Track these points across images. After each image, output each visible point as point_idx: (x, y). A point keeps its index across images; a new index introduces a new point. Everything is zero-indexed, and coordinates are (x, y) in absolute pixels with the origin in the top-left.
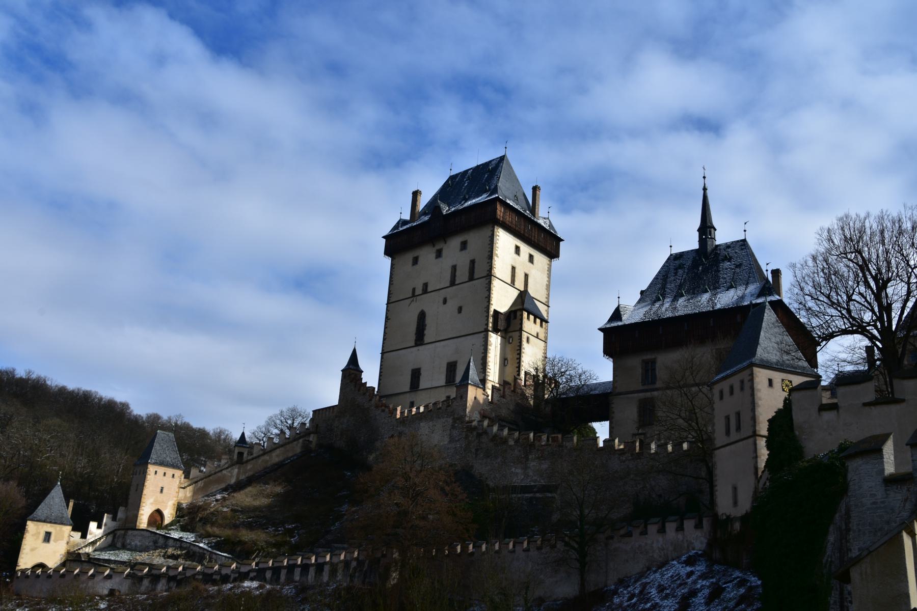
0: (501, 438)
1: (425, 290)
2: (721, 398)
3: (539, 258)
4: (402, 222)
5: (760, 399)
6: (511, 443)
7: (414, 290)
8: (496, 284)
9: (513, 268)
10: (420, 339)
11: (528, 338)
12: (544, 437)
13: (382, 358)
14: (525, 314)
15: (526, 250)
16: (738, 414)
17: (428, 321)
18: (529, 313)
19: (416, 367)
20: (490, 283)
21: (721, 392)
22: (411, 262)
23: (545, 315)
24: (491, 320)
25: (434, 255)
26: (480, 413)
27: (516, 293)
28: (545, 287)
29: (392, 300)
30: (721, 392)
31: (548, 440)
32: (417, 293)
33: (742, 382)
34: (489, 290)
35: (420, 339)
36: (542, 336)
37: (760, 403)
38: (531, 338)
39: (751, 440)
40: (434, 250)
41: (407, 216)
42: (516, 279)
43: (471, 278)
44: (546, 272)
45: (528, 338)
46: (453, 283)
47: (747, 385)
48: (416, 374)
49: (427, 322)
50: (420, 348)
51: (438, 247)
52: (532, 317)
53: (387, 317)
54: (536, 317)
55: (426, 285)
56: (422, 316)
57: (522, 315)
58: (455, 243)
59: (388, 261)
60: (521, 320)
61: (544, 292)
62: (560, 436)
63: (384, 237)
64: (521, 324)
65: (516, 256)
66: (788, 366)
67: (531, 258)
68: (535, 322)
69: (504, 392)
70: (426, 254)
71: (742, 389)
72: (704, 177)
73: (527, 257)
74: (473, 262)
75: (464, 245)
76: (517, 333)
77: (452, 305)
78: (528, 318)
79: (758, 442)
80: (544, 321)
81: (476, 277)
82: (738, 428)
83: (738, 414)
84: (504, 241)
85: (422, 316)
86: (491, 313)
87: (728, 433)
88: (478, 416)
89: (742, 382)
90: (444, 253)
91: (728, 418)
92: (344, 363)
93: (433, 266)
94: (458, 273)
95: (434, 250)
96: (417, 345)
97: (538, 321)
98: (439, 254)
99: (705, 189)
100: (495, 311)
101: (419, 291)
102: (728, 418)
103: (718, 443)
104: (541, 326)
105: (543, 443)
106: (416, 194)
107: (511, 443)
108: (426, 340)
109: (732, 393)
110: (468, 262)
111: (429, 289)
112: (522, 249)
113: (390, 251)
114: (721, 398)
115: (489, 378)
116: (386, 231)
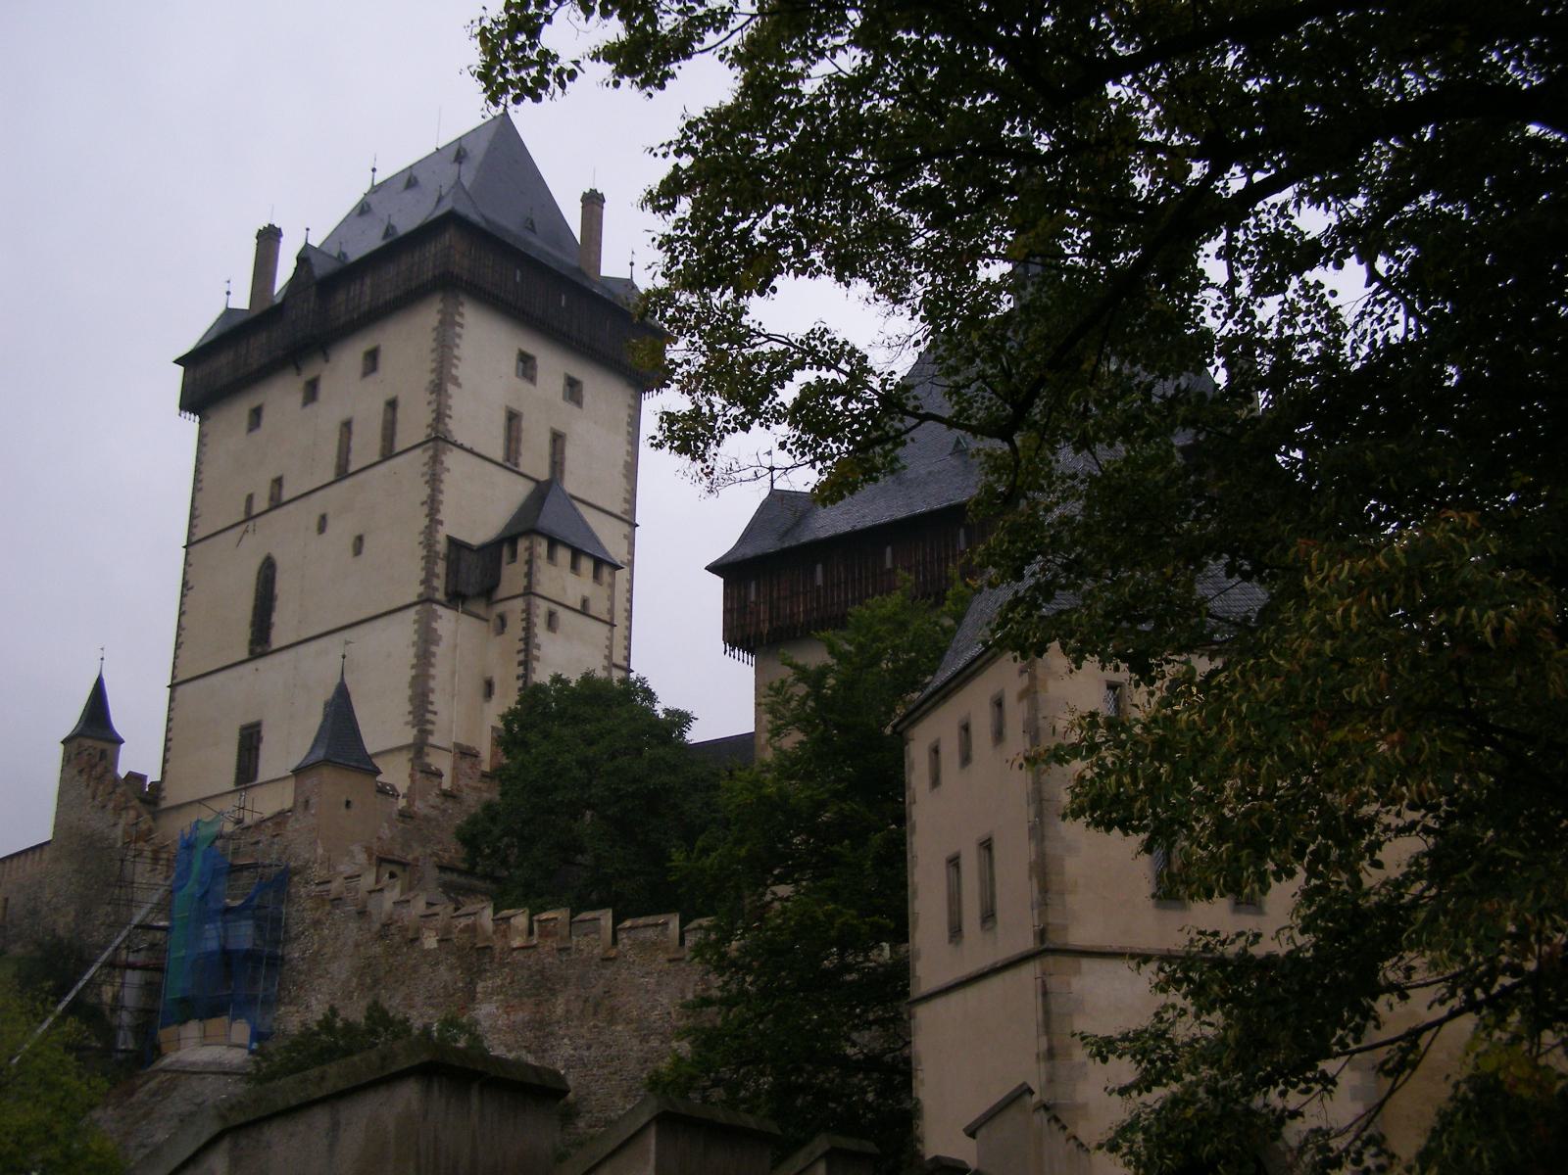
0: (403, 929)
1: (276, 503)
2: (935, 781)
3: (603, 391)
4: (229, 312)
6: (430, 942)
7: (250, 498)
8: (453, 459)
9: (513, 418)
10: (260, 641)
11: (551, 615)
12: (520, 920)
13: (171, 699)
14: (542, 548)
15: (553, 365)
16: (987, 845)
17: (283, 585)
18: (553, 543)
19: (251, 719)
20: (435, 460)
21: (935, 751)
22: (244, 424)
23: (616, 551)
24: (441, 568)
25: (299, 397)
26: (368, 850)
27: (521, 490)
28: (620, 468)
29: (200, 534)
30: (935, 751)
31: (531, 932)
32: (256, 510)
33: (999, 704)
34: (434, 481)
35: (260, 641)
36: (598, 607)
38: (562, 613)
39: (1029, 972)
41: (242, 301)
42: (524, 449)
43: (388, 453)
44: (624, 428)
45: (551, 615)
46: (343, 473)
47: (1016, 714)
48: (250, 740)
49: (277, 591)
50: (261, 663)
51: (308, 374)
52: (563, 555)
53: (185, 584)
54: (577, 553)
55: (278, 482)
56: (267, 573)
57: (530, 550)
58: (349, 357)
59: (191, 424)
60: (530, 563)
61: (623, 483)
62: (561, 914)
64: (529, 575)
65: (523, 385)
67: (573, 387)
68: (574, 567)
69: (455, 778)
70: (281, 396)
71: (999, 735)
73: (559, 385)
74: (392, 405)
75: (372, 359)
77: (341, 531)
78: (551, 556)
79: (1053, 983)
80: (603, 565)
81: (399, 447)
82: (988, 916)
83: (987, 845)
84: (486, 346)
85: (267, 573)
86: (442, 547)
87: (956, 932)
88: (362, 857)
89: (999, 704)
91: (954, 862)
92: (70, 717)
93: (295, 424)
94: (356, 443)
96: (254, 656)
97: (586, 565)
98: (311, 392)
100: (452, 542)
102: (954, 862)
103: (927, 974)
104: (596, 576)
105: (517, 942)
106: (269, 237)
107: (430, 942)
108: (278, 639)
109: (966, 759)
111: (286, 497)
112: (540, 362)
113: (198, 399)
114: (935, 781)
115: (432, 740)
116: (188, 344)
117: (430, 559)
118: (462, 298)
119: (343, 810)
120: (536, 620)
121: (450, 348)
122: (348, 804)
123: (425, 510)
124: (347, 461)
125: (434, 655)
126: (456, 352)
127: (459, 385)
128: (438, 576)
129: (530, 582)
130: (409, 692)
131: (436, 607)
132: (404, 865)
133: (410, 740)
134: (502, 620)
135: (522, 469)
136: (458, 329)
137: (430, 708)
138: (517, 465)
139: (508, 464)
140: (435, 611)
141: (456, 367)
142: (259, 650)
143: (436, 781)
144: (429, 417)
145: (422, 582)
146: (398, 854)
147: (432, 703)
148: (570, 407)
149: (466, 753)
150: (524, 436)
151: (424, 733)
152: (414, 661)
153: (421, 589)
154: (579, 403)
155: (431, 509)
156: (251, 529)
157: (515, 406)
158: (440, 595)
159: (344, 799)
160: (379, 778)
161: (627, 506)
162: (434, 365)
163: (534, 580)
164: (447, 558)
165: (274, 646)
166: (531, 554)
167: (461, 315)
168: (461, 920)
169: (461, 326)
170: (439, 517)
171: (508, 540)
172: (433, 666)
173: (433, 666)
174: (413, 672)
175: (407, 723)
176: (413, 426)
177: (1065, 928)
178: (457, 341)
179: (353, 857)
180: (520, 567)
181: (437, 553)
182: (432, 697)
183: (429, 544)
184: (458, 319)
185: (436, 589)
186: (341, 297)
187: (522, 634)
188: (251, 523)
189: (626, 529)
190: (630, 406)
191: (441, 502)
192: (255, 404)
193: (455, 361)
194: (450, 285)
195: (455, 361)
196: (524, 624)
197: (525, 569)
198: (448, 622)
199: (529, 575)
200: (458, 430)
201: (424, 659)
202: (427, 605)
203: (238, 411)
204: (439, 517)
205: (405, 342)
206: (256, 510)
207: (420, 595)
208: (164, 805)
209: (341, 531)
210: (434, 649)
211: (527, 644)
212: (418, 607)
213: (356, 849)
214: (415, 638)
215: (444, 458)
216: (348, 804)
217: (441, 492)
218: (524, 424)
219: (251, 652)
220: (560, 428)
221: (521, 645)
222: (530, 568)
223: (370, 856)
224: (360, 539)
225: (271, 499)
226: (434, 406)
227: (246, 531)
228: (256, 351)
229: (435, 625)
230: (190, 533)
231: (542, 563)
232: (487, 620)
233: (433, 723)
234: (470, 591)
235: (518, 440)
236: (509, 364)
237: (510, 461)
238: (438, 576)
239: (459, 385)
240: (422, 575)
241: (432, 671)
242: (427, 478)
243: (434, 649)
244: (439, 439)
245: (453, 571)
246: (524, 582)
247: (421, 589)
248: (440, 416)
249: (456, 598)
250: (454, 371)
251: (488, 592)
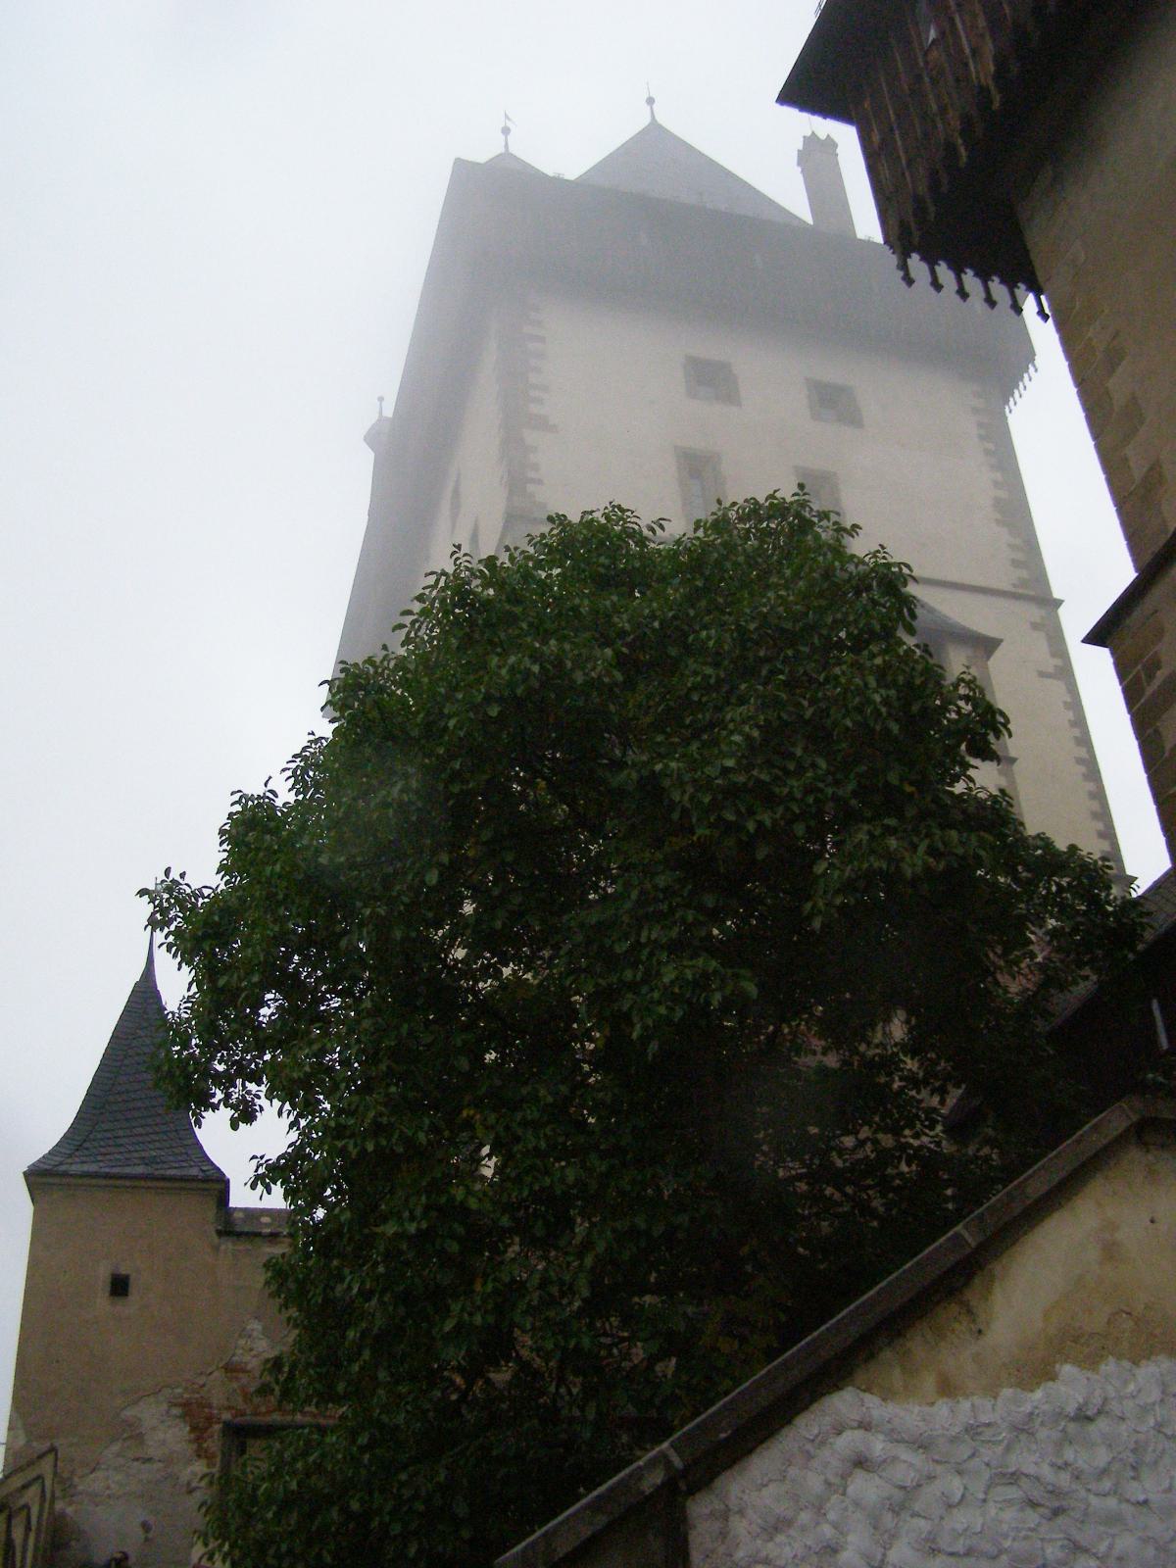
26: (194, 1414)
119: (102, 1302)
122: (119, 1286)
159: (103, 1272)
161: (1024, 574)
169: (542, 340)
179: (139, 1438)
189: (1035, 613)
190: (976, 411)
216: (119, 1286)
223: (199, 1432)
250: (534, 409)
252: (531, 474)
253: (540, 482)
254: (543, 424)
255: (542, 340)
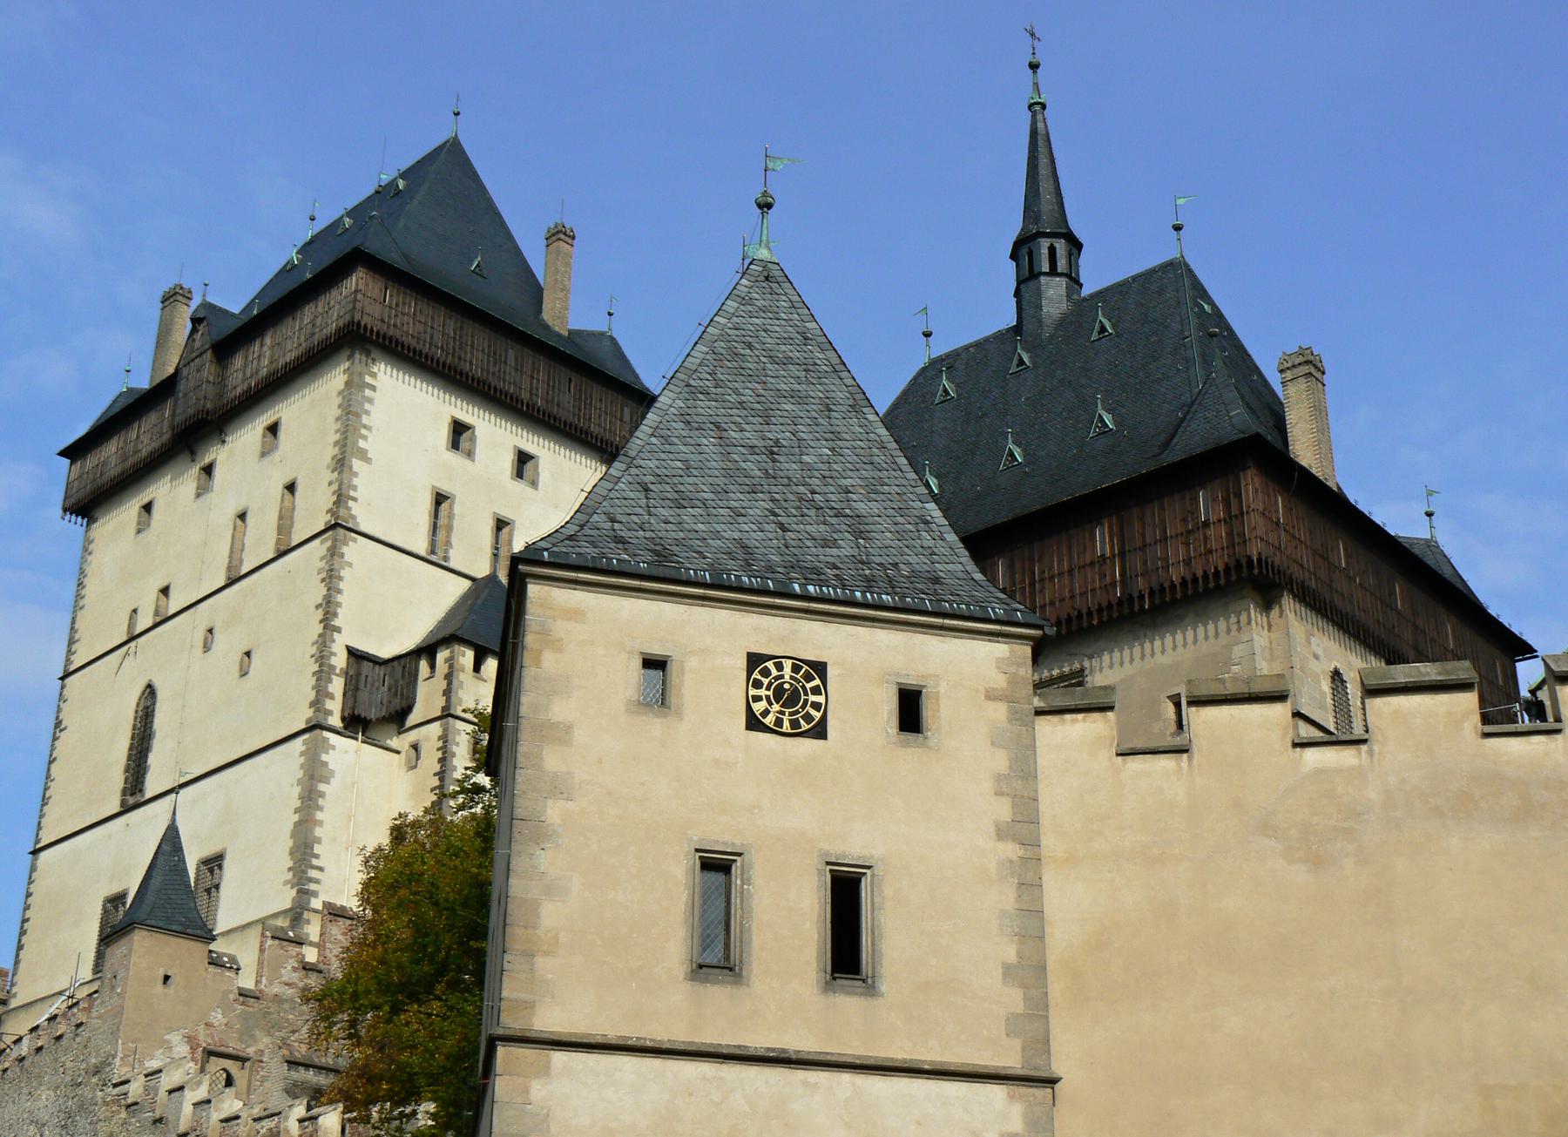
5: (559, 788)
8: (355, 551)
9: (440, 499)
14: (468, 656)
15: (498, 437)
20: (334, 552)
24: (337, 686)
26: (191, 1040)
34: (331, 578)
37: (554, 812)
40: (195, 470)
53: (58, 724)
55: (165, 591)
63: (63, 453)
65: (455, 459)
66: (814, 574)
70: (172, 492)
72: (1034, 67)
73: (508, 461)
76: (436, 728)
77: (228, 647)
84: (405, 409)
86: (340, 660)
88: (182, 1049)
90: (218, 472)
95: (195, 470)
96: (126, 809)
99: (1036, 108)
100: (352, 653)
101: (145, 621)
110: (278, 490)
117: (323, 673)
118: (375, 353)
120: (455, 749)
121: (358, 416)
122: (167, 978)
123: (320, 614)
124: (241, 561)
125: (322, 795)
126: (365, 419)
127: (367, 460)
128: (332, 697)
129: (448, 700)
130: (290, 843)
131: (326, 734)
132: (242, 1060)
133: (288, 904)
134: (415, 747)
135: (452, 565)
136: (368, 392)
137: (315, 862)
138: (446, 559)
139: (433, 558)
140: (326, 740)
141: (365, 438)
142: (131, 801)
143: (293, 950)
144: (328, 500)
145: (312, 704)
146: (233, 1046)
147: (317, 856)
148: (520, 487)
149: (335, 913)
150: (456, 523)
151: (304, 894)
152: (298, 804)
153: (309, 713)
154: (534, 484)
155: (327, 613)
156: (132, 651)
157: (445, 487)
158: (335, 721)
159: (161, 973)
160: (213, 947)
162: (338, 437)
163: (453, 698)
164: (346, 673)
165: (149, 794)
166: (451, 667)
167: (374, 375)
168: (264, 1123)
169: (373, 388)
170: (336, 622)
171: (427, 650)
172: (321, 809)
173: (321, 809)
174: (296, 818)
175: (286, 883)
176: (312, 513)
177: (530, 1006)
178: (367, 406)
180: (439, 683)
181: (332, 668)
182: (317, 849)
183: (322, 657)
184: (368, 379)
185: (329, 713)
186: (238, 361)
187: (437, 768)
188: (133, 644)
191: (339, 605)
192: (146, 501)
193: (363, 431)
194: (355, 340)
195: (363, 431)
196: (440, 755)
197: (444, 684)
198: (344, 752)
199: (447, 693)
200: (363, 515)
201: (310, 799)
202: (318, 731)
203: (125, 513)
204: (336, 622)
205: (308, 411)
206: (138, 630)
207: (308, 721)
208: (14, 1003)
209: (228, 647)
210: (322, 787)
211: (442, 780)
212: (306, 736)
213: (175, 1038)
214: (300, 774)
215: (345, 549)
216: (167, 978)
217: (339, 591)
218: (457, 509)
219: (123, 803)
220: (506, 513)
221: (436, 782)
222: (450, 684)
223: (193, 1050)
224: (248, 654)
225: (157, 613)
226: (335, 487)
227: (127, 653)
228: (147, 435)
229: (324, 757)
230: (68, 661)
231: (465, 676)
232: (398, 752)
233: (317, 881)
234: (373, 714)
235: (450, 528)
236: (444, 432)
237: (435, 557)
238: (332, 697)
239: (367, 460)
240: (312, 695)
241: (319, 816)
242: (324, 575)
243: (322, 787)
244: (338, 527)
245: (352, 690)
246: (442, 702)
247: (309, 713)
248: (341, 498)
249: (355, 724)
250: (361, 443)
251: (398, 718)
252: (352, 493)
253: (355, 499)
254: (364, 456)
255: (373, 388)
